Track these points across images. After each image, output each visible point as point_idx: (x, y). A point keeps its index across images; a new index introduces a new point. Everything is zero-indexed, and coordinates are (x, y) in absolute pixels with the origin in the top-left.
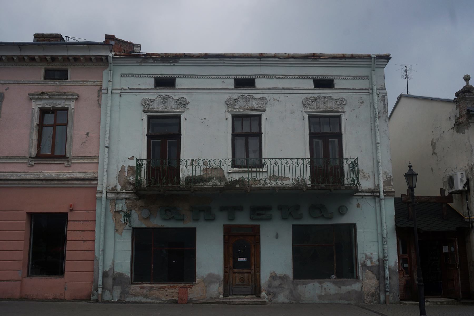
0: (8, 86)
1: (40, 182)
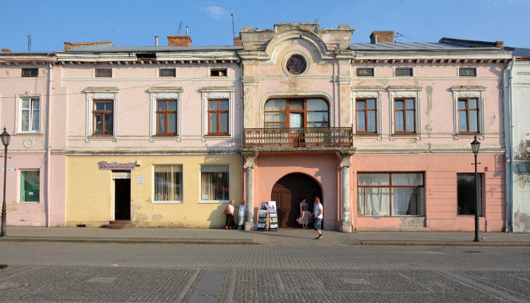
0: (434, 82)
1: (466, 152)
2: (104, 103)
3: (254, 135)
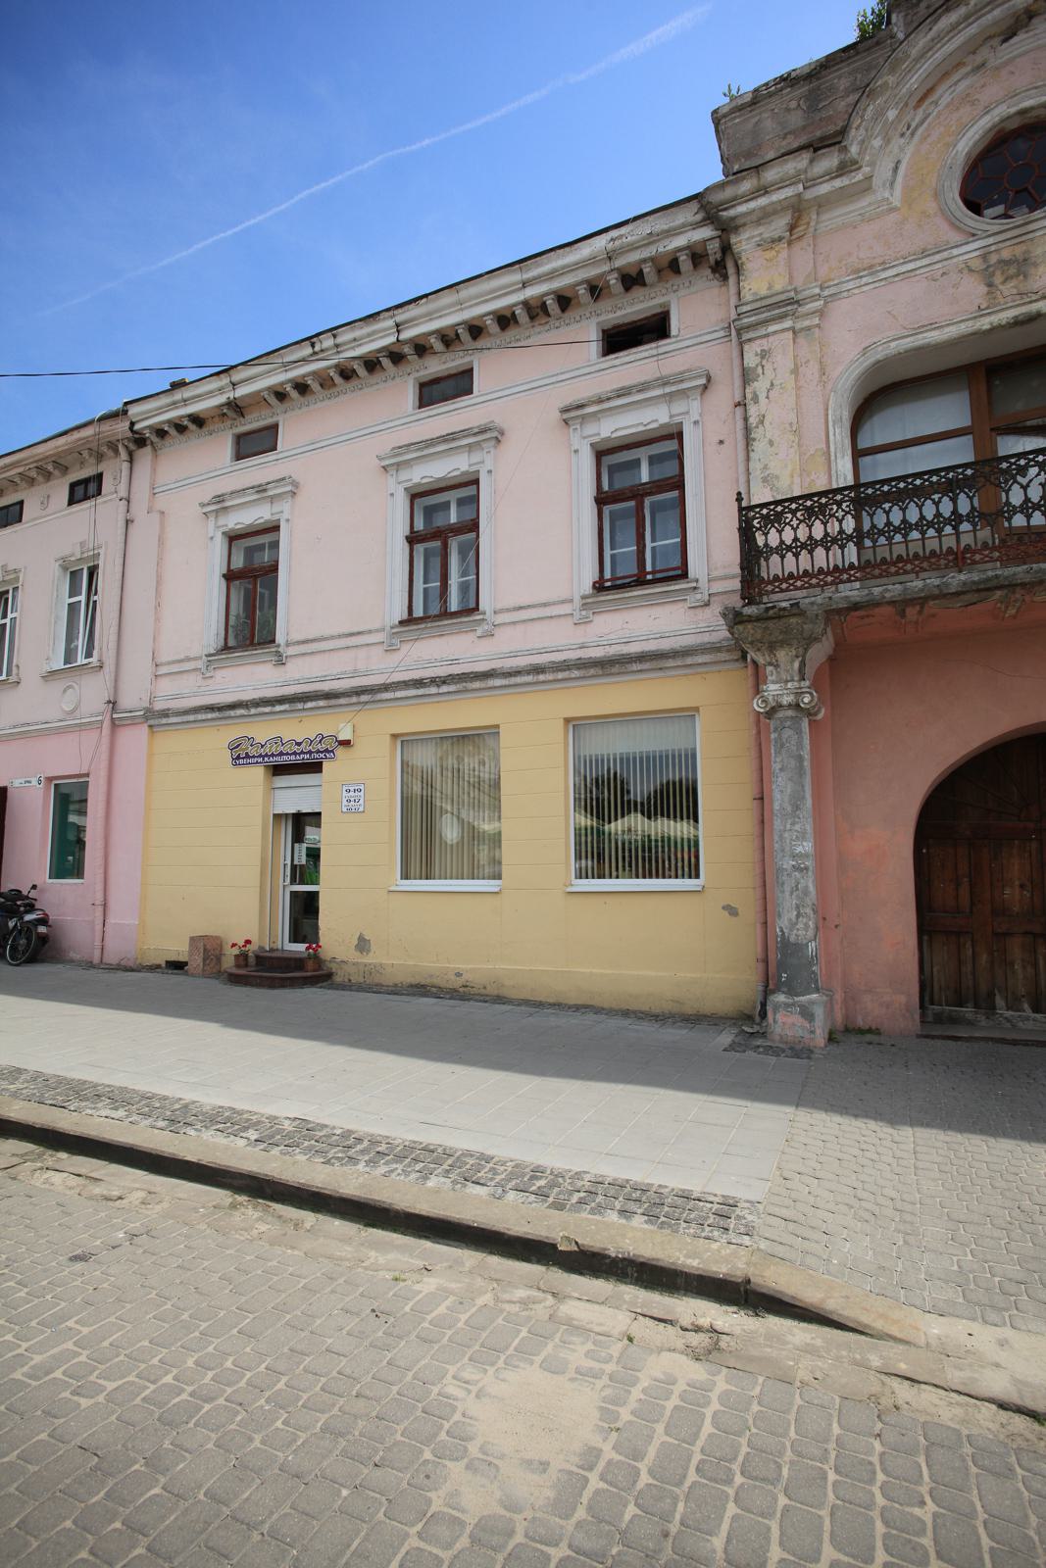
2: (263, 545)
3: (795, 530)
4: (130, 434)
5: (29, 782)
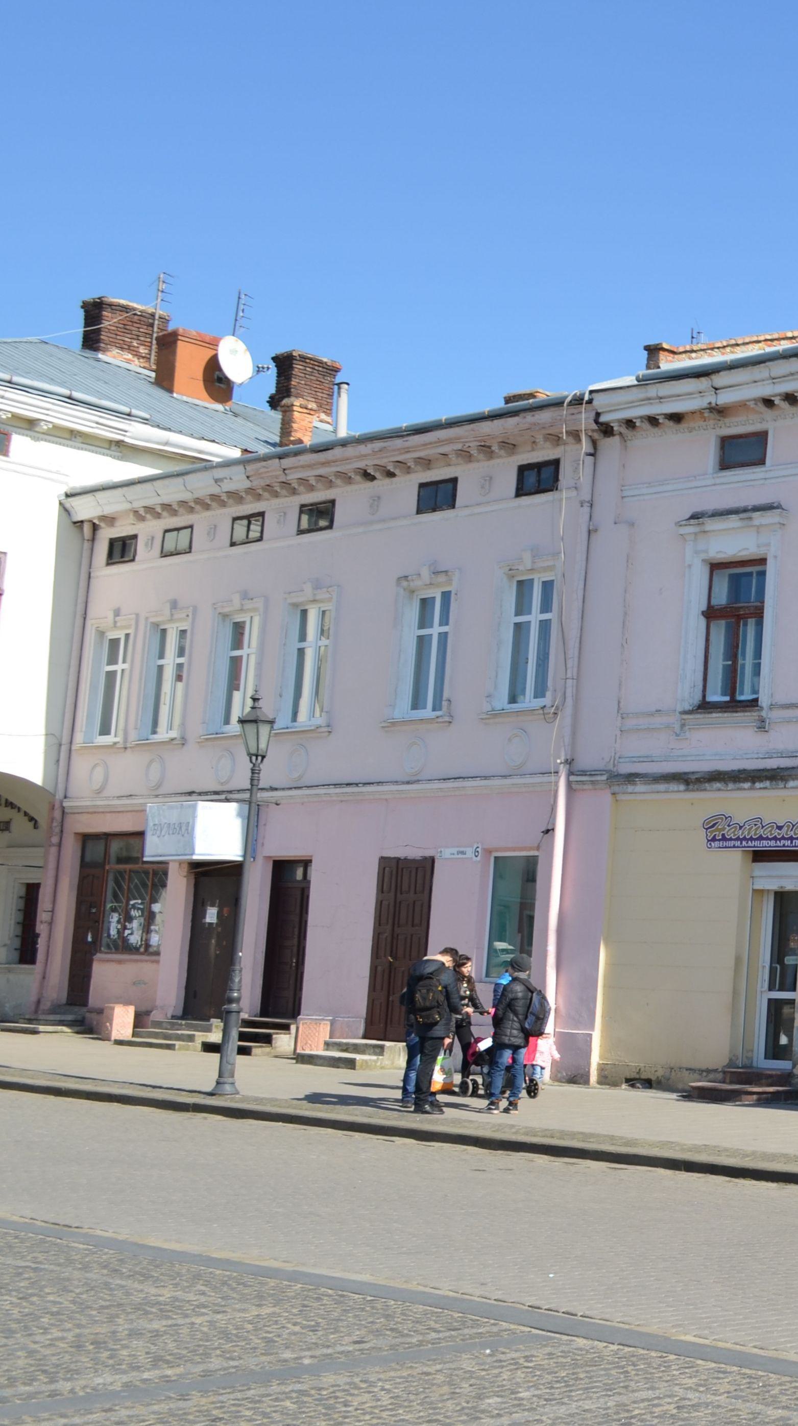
2: (751, 574)
4: (595, 427)
5: (463, 853)
